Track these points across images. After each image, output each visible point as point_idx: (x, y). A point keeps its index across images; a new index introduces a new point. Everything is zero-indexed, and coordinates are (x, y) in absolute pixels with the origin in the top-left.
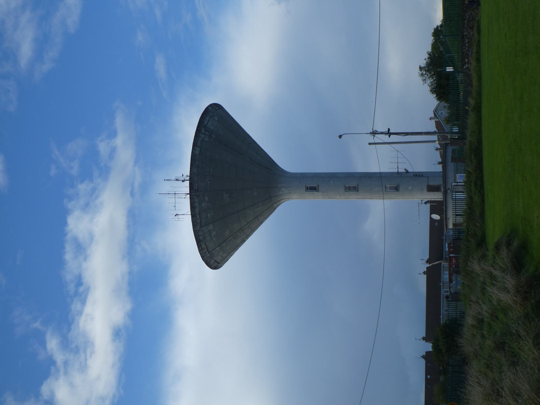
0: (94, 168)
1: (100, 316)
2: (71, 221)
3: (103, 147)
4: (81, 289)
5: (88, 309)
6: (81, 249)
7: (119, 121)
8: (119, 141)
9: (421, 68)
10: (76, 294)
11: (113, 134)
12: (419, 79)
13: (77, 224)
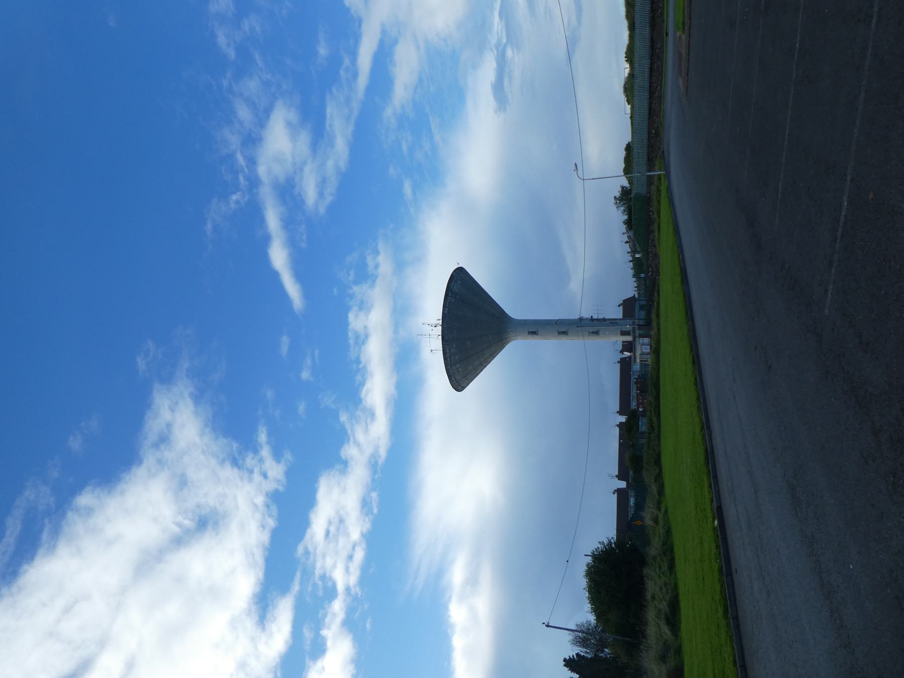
0: (365, 275)
1: (377, 390)
2: (351, 316)
3: (370, 261)
4: (361, 366)
5: (368, 385)
6: (362, 339)
7: (381, 246)
8: (381, 258)
9: (615, 198)
10: (358, 370)
11: (377, 252)
12: (614, 207)
13: (356, 321)
